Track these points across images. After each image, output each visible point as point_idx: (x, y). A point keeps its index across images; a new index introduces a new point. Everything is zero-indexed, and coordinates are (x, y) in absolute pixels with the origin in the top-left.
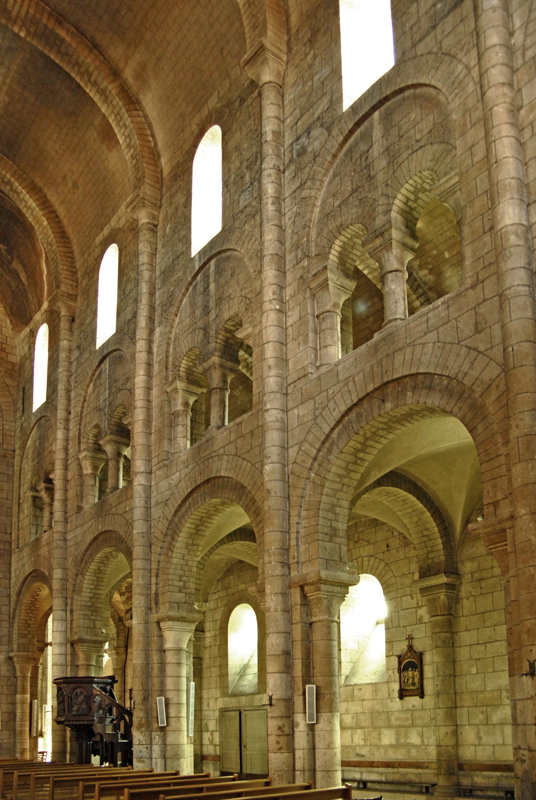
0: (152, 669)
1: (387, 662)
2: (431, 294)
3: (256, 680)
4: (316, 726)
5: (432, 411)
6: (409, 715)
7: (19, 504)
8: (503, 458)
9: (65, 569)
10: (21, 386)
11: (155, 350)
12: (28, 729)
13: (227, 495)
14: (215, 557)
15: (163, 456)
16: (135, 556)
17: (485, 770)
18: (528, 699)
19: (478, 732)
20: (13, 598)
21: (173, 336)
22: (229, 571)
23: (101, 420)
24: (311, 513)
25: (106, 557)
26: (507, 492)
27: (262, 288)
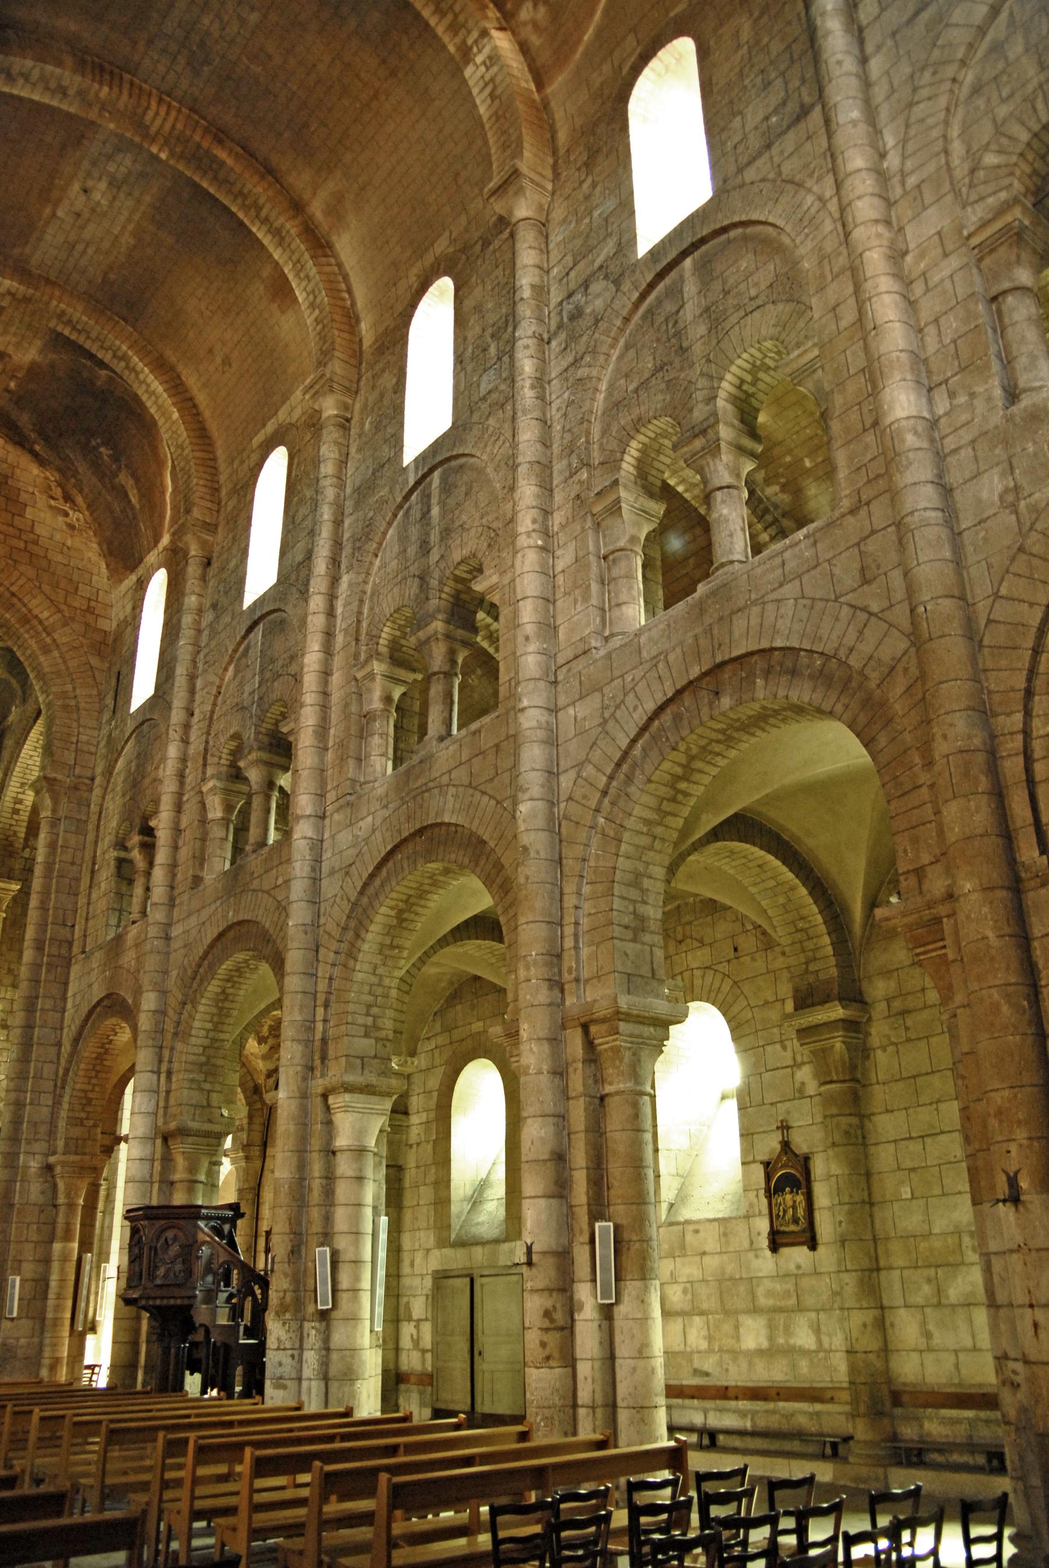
0: (310, 1190)
1: (745, 1175)
2: (786, 523)
3: (502, 1212)
4: (616, 1309)
5: (799, 710)
6: (790, 1286)
7: (93, 872)
8: (924, 790)
9: (163, 993)
10: (115, 669)
11: (339, 610)
12: (68, 1315)
13: (453, 856)
14: (430, 970)
15: (346, 787)
16: (288, 967)
17: (944, 1406)
18: (1012, 1251)
19: (924, 1323)
20: (66, 1048)
21: (369, 588)
22: (455, 996)
23: (244, 727)
24: (600, 888)
25: (238, 970)
26: (938, 852)
27: (515, 513)
